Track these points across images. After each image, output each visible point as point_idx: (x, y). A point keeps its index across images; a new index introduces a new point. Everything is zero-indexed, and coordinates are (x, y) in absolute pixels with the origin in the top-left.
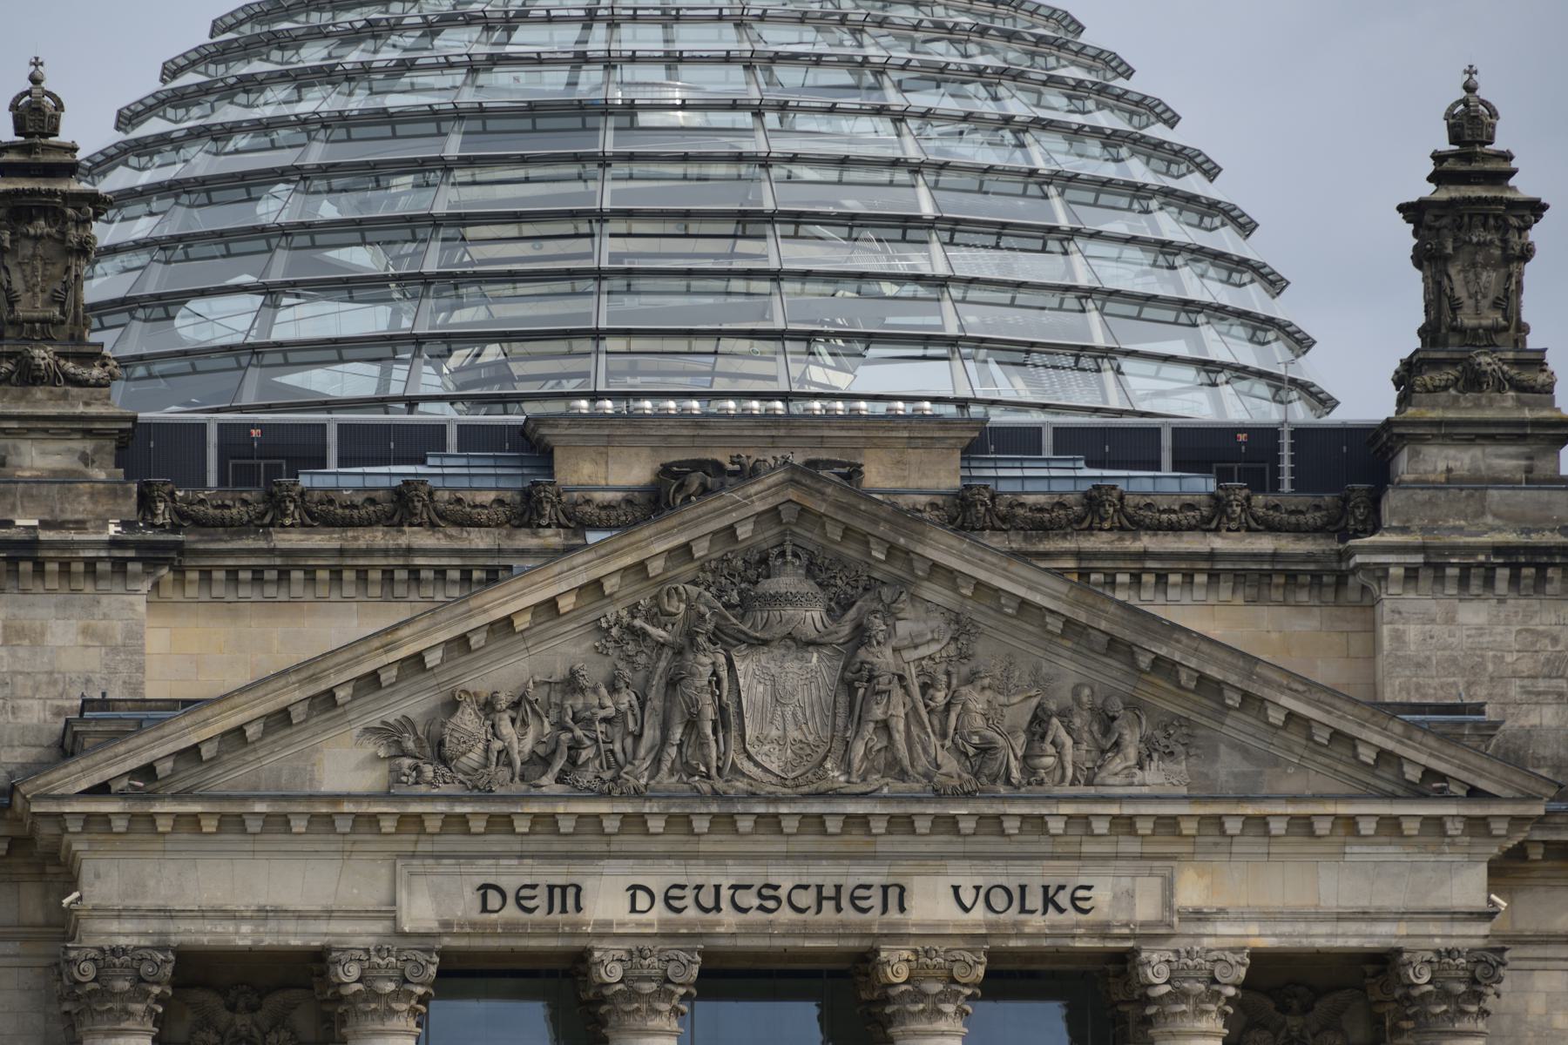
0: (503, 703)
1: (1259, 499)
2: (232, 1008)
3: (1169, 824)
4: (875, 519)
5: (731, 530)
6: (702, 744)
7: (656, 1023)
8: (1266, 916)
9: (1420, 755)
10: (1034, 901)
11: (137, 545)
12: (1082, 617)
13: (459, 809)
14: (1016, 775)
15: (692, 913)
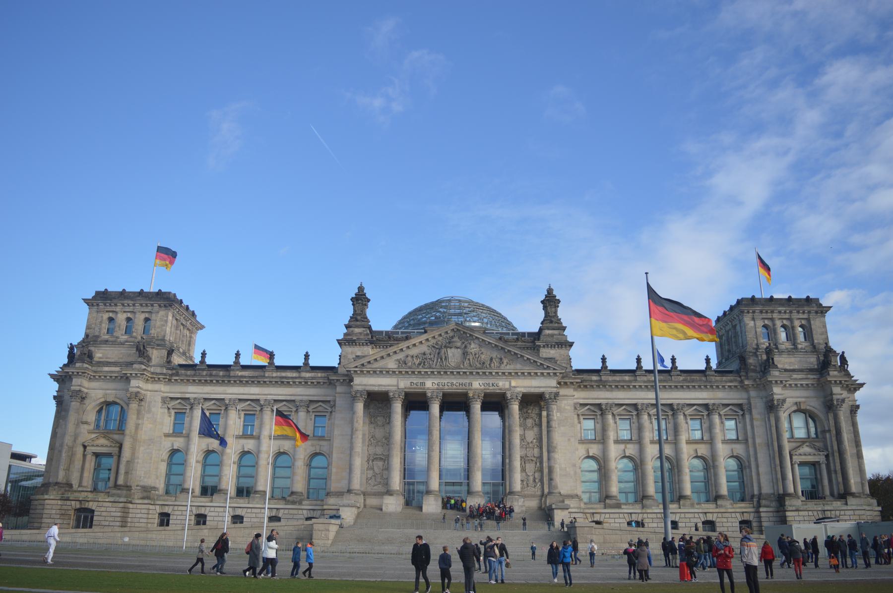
0: (414, 356)
1: (523, 338)
2: (379, 403)
3: (510, 373)
4: (467, 330)
5: (447, 333)
6: (443, 362)
7: (435, 402)
8: (525, 387)
9: (546, 364)
10: (491, 385)
11: (369, 341)
12: (497, 344)
13: (407, 370)
14: (488, 367)
15: (441, 386)
